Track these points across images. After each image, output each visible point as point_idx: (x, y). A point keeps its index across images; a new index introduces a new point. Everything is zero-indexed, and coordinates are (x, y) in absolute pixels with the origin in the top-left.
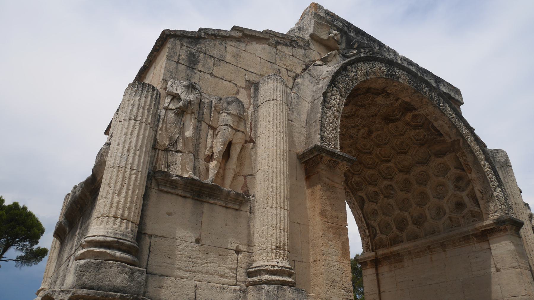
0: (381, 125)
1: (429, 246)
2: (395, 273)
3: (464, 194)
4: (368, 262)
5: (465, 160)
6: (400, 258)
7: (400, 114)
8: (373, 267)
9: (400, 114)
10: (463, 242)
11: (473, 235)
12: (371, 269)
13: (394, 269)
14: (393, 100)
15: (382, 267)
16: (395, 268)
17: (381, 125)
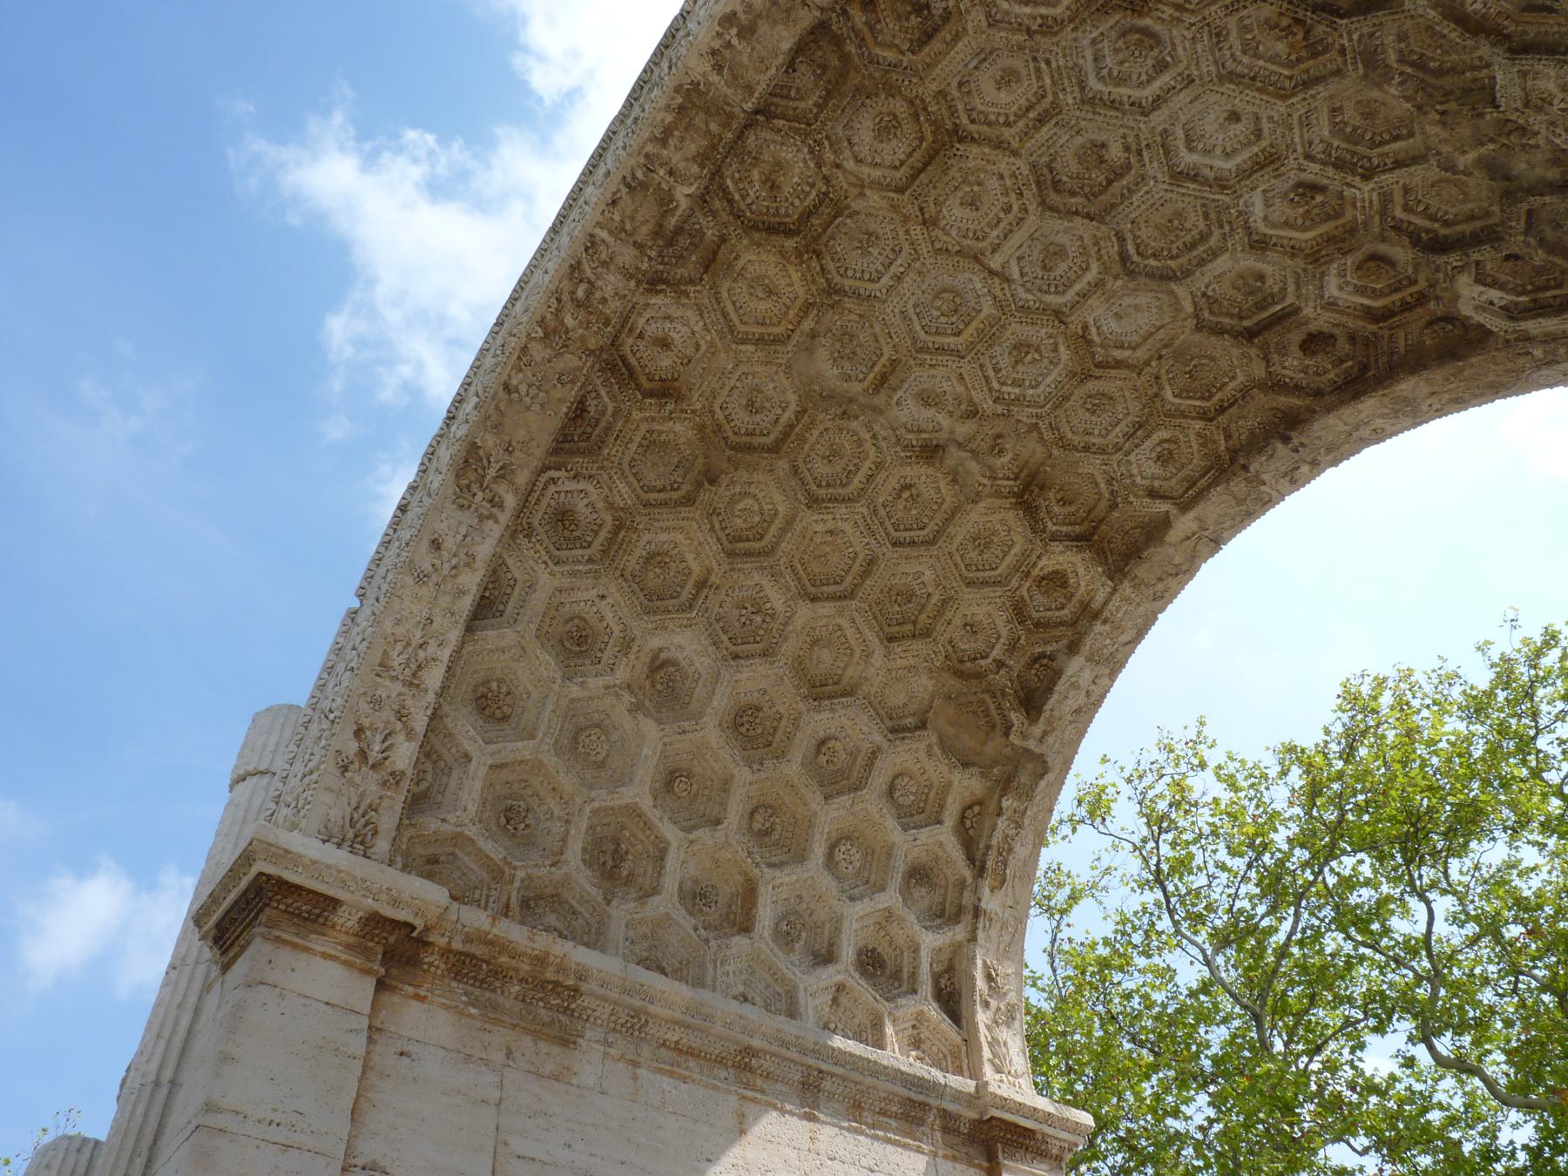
0: (985, 481)
1: (749, 1052)
2: (501, 1086)
3: (931, 942)
4: (347, 919)
5: (1007, 836)
6: (563, 1018)
7: (1064, 529)
8: (367, 972)
9: (1064, 529)
10: (894, 1123)
11: (945, 1114)
12: (335, 971)
13: (498, 1057)
14: (1146, 483)
15: (414, 1003)
16: (509, 1054)
17: (985, 481)
